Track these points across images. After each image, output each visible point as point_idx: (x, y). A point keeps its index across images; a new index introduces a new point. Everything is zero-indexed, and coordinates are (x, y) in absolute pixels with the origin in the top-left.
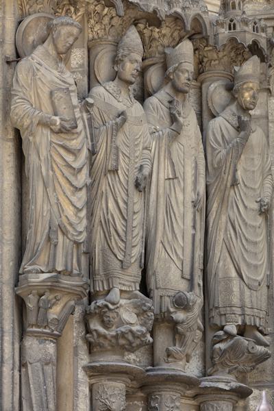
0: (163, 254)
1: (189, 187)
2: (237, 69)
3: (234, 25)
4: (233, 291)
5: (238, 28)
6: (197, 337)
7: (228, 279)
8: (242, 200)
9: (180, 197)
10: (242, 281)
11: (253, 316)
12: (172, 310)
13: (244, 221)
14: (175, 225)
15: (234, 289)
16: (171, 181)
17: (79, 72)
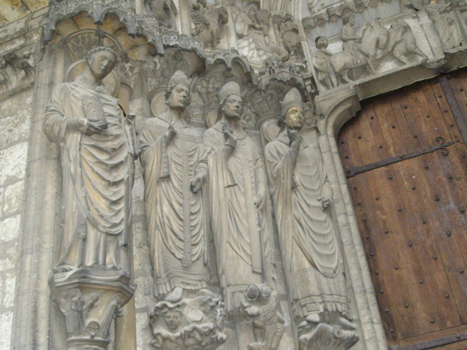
0: (231, 252)
1: (250, 192)
2: (281, 102)
3: (273, 70)
4: (309, 282)
5: (276, 71)
6: (279, 331)
7: (303, 271)
8: (305, 201)
9: (242, 200)
10: (316, 271)
11: (333, 302)
12: (246, 304)
13: (309, 217)
14: (239, 224)
15: (310, 279)
16: (231, 188)
17: (139, 114)
